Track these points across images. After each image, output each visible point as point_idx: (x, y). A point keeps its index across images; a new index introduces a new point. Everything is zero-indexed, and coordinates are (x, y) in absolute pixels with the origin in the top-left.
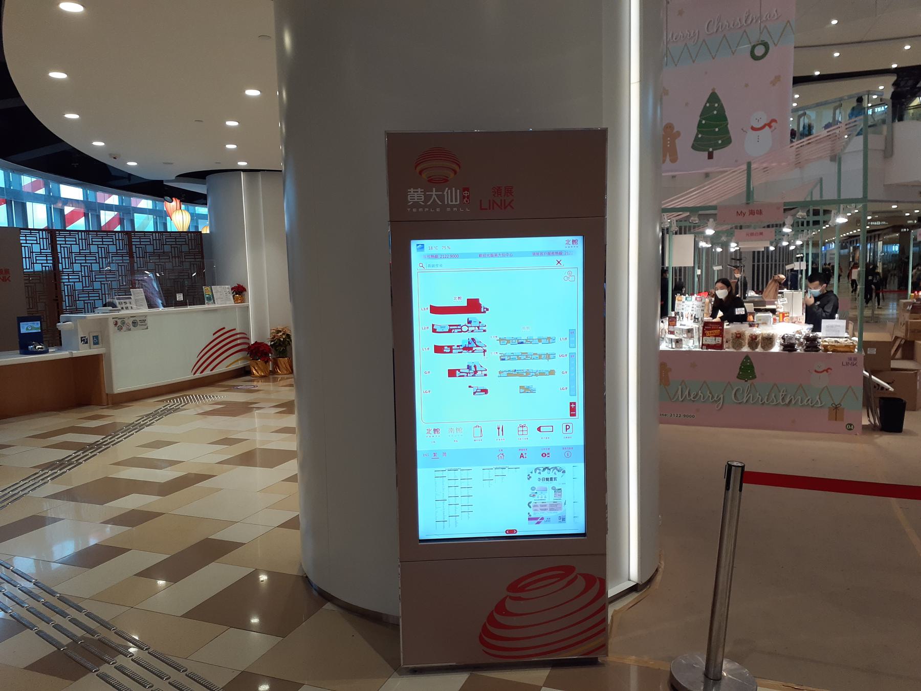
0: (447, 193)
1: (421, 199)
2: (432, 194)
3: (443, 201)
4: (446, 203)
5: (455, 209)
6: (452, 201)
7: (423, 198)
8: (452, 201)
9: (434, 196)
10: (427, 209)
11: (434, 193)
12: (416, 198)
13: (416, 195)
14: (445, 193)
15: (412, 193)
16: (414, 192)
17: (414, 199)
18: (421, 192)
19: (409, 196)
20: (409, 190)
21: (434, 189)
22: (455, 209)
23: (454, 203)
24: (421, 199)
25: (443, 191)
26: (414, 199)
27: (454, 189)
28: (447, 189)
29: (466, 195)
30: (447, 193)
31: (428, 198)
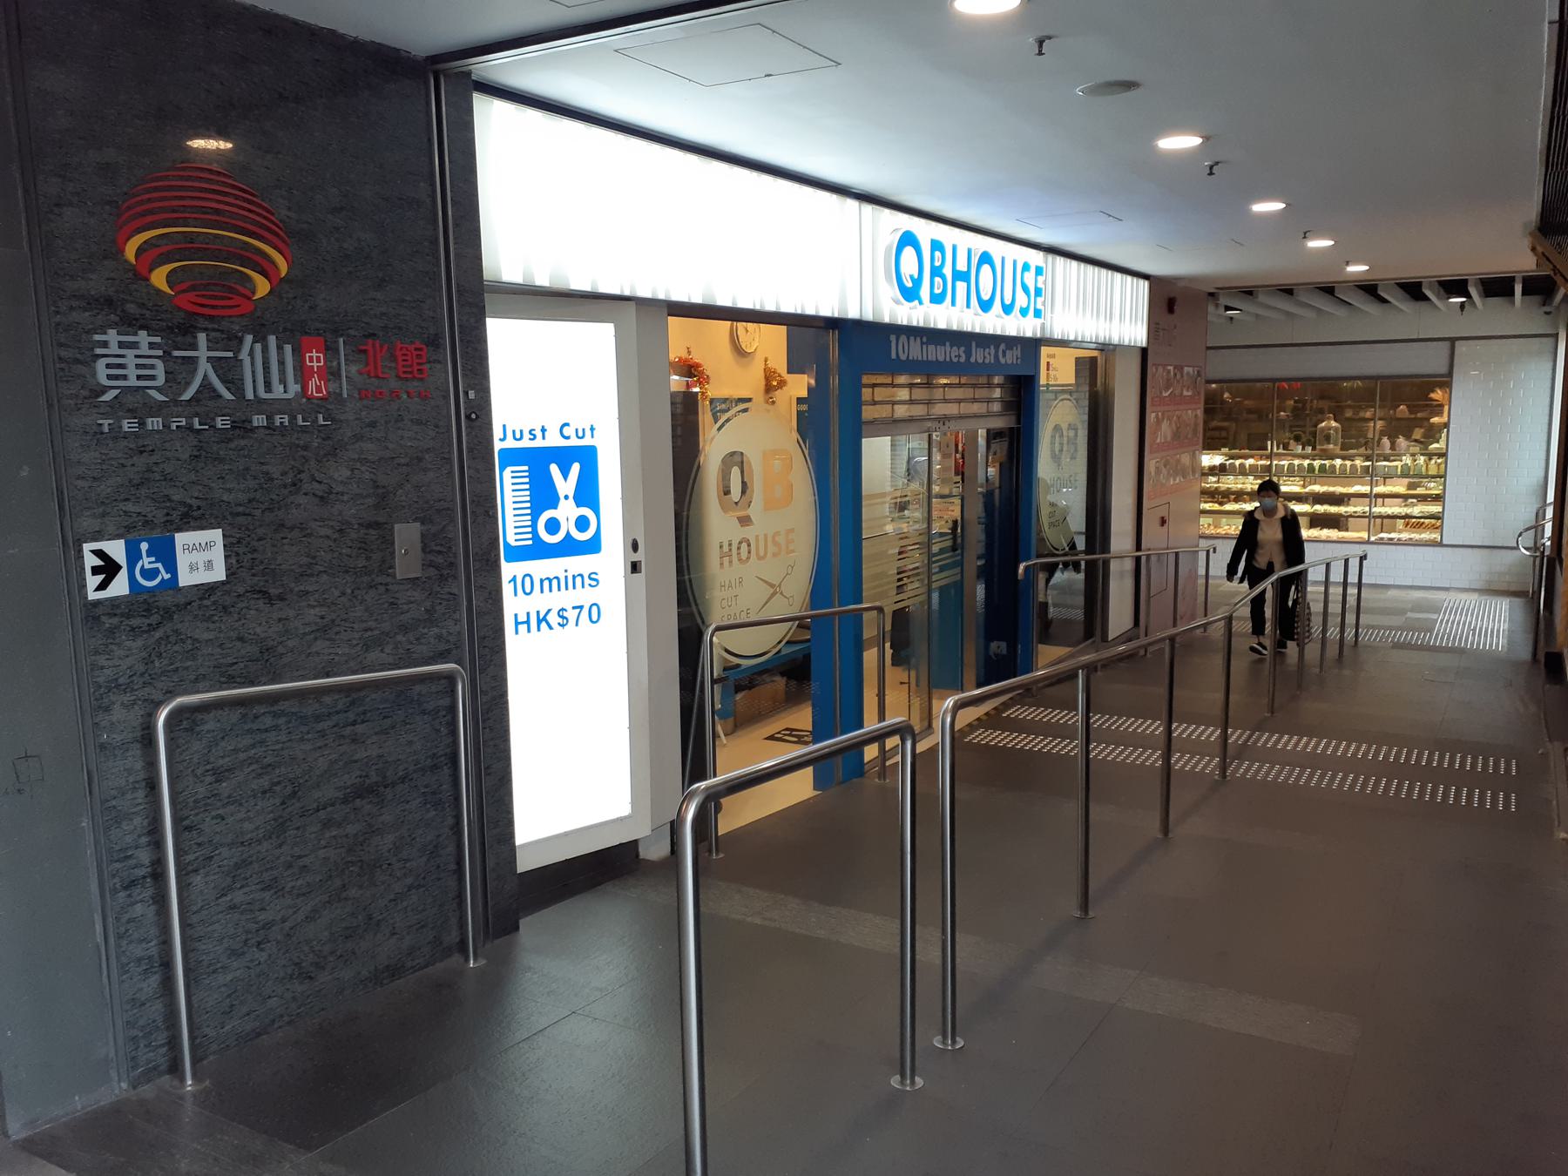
8: (268, 387)
12: (132, 372)
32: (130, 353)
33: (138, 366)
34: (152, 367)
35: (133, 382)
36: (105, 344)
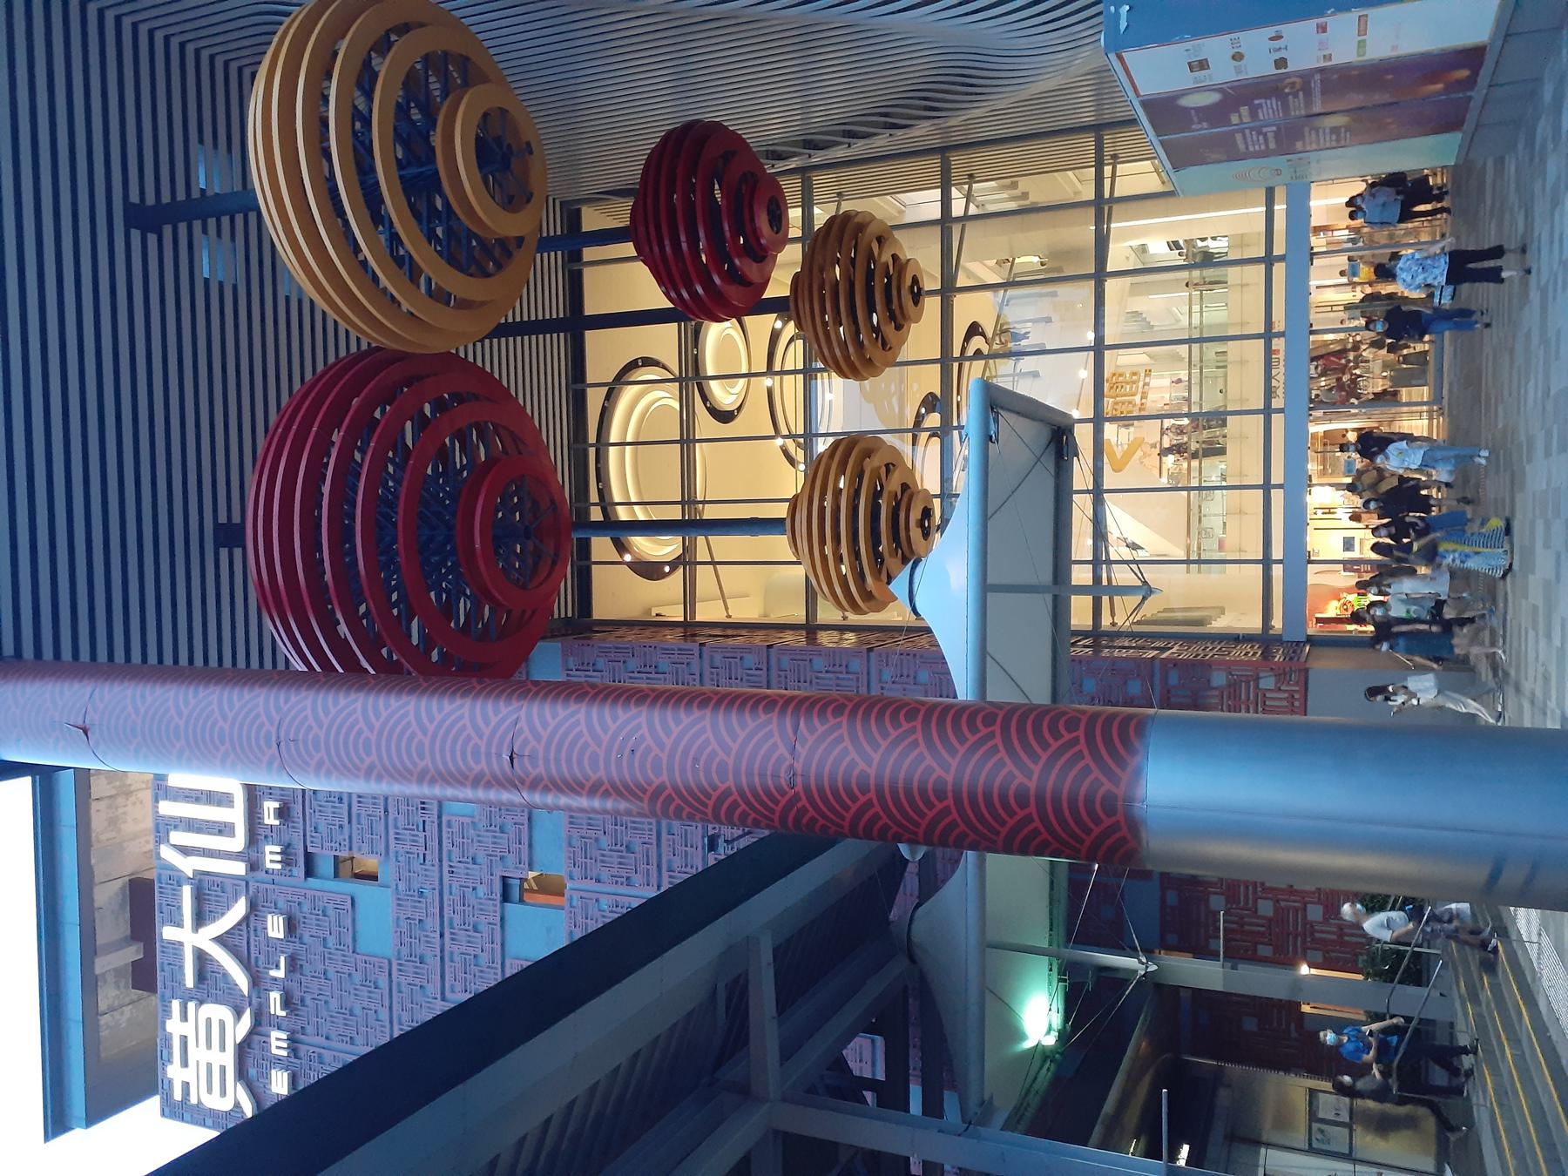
0: (185, 851)
1: (222, 1024)
4: (239, 868)
10: (275, 997)
14: (188, 866)
16: (185, 1064)
17: (223, 1069)
23: (236, 815)
24: (222, 1024)
26: (223, 1069)
30: (185, 851)
31: (209, 981)
34: (209, 1021)
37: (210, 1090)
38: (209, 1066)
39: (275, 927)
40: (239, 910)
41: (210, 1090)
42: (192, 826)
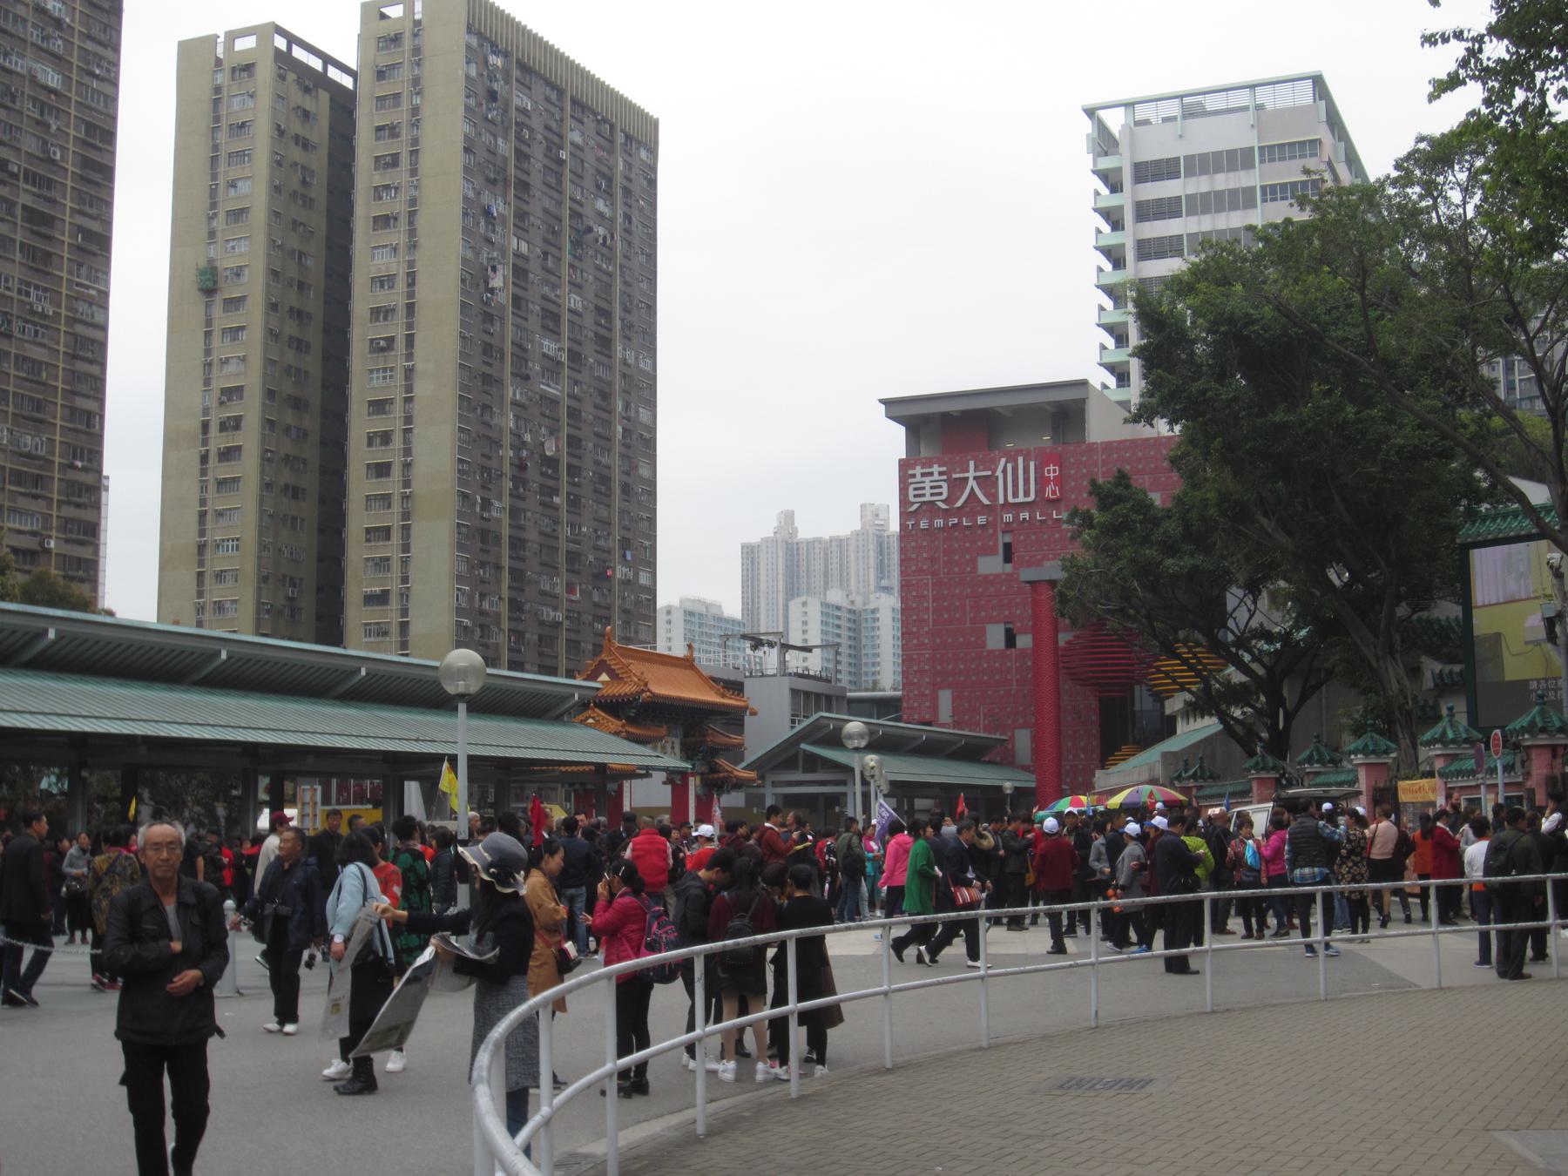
0: (1005, 471)
1: (941, 494)
2: (967, 478)
3: (993, 496)
4: (1001, 501)
5: (1025, 515)
6: (1015, 494)
7: (945, 490)
8: (1015, 494)
9: (972, 483)
10: (956, 521)
11: (971, 474)
12: (928, 491)
13: (927, 485)
14: (999, 473)
15: (918, 478)
16: (923, 475)
17: (923, 495)
18: (941, 473)
19: (911, 488)
20: (910, 472)
21: (972, 463)
22: (1025, 515)
23: (1021, 499)
24: (941, 494)
25: (994, 471)
26: (923, 495)
27: (1020, 460)
28: (1003, 461)
29: (1052, 475)
30: (1005, 471)
31: (957, 485)
32: (927, 479)
33: (932, 488)
34: (940, 487)
35: (928, 498)
36: (914, 476)
37: (915, 489)
38: (924, 488)
39: (981, 520)
40: (986, 501)
41: (915, 489)
42: (1015, 470)
